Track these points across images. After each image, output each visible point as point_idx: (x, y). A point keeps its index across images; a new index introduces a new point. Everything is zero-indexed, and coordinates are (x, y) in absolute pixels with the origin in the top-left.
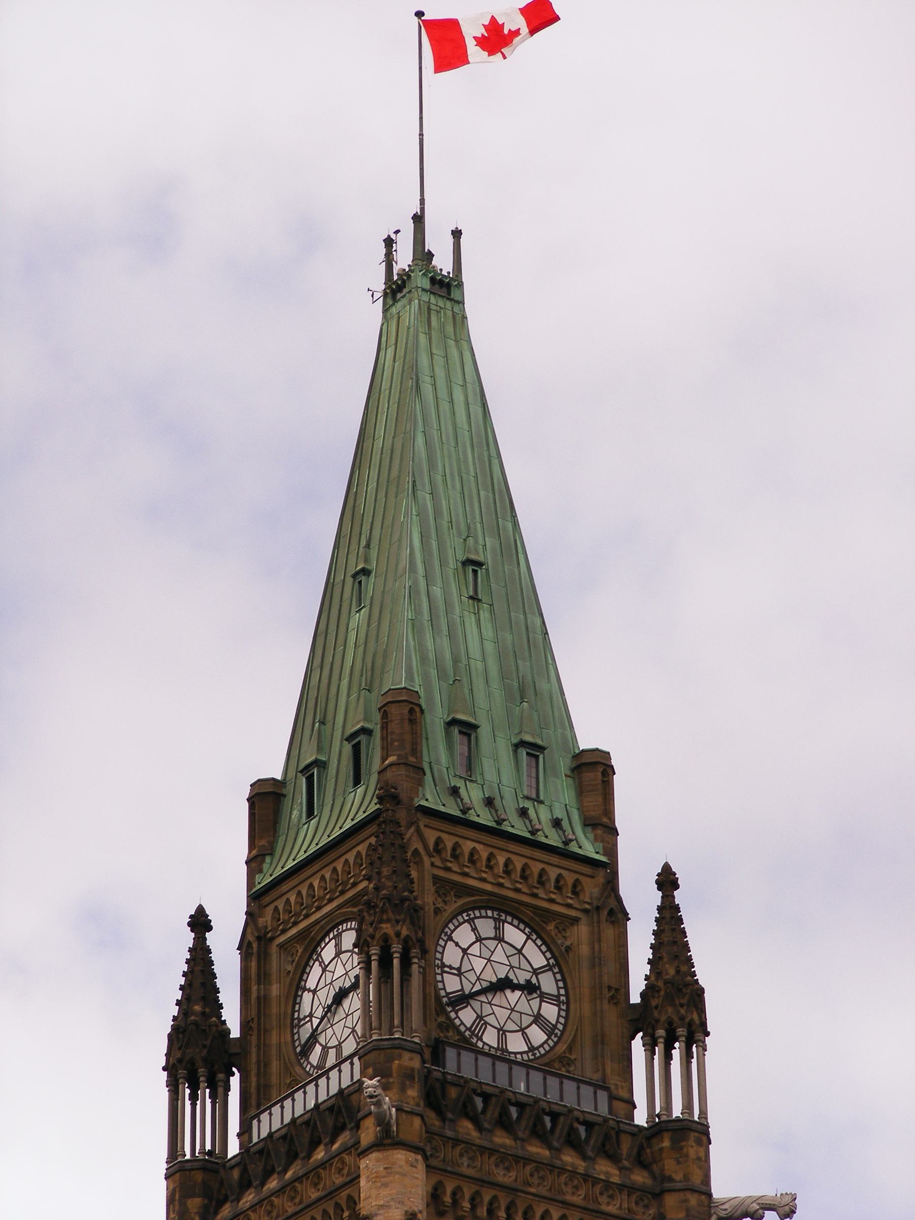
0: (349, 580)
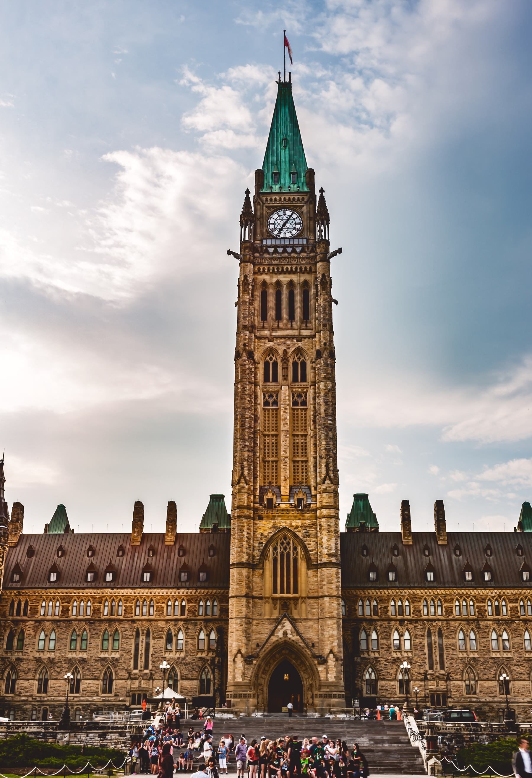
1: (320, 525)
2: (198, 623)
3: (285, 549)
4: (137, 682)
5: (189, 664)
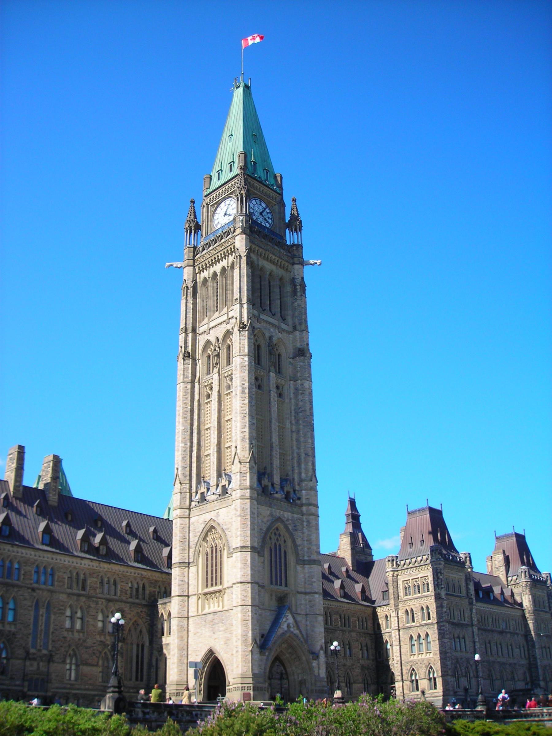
0: (227, 137)
1: (308, 522)
2: (100, 603)
3: (277, 540)
4: (35, 664)
5: (90, 647)
